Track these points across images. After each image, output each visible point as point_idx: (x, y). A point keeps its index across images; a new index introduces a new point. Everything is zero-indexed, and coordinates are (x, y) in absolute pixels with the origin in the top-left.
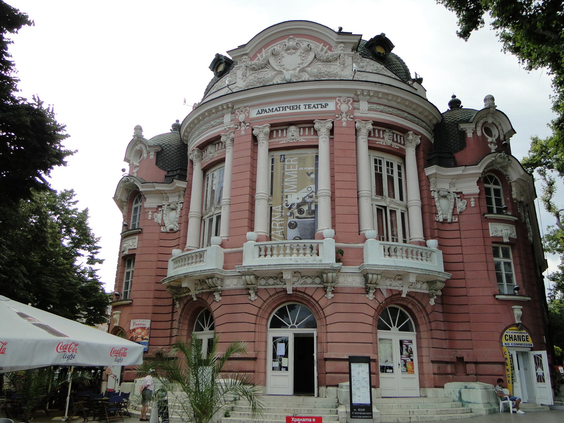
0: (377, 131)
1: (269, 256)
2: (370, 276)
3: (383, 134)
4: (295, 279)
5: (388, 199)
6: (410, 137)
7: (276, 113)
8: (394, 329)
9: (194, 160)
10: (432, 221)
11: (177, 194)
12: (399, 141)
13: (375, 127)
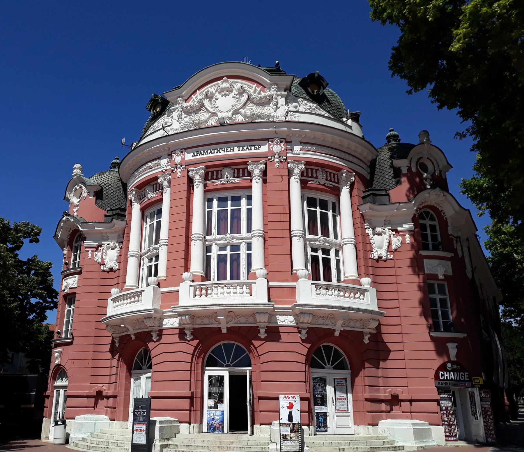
0: (310, 170)
1: (203, 296)
3: (316, 173)
10: (366, 259)
12: (333, 180)
13: (308, 167)
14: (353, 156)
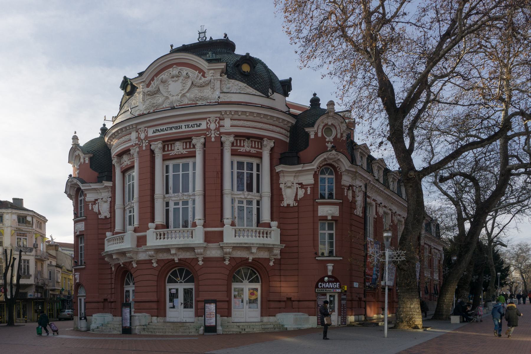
1: (162, 239)
4: (180, 253)
5: (246, 193)
6: (265, 143)
7: (166, 132)
9: (116, 165)
11: (106, 190)
12: (257, 146)
14: (273, 125)
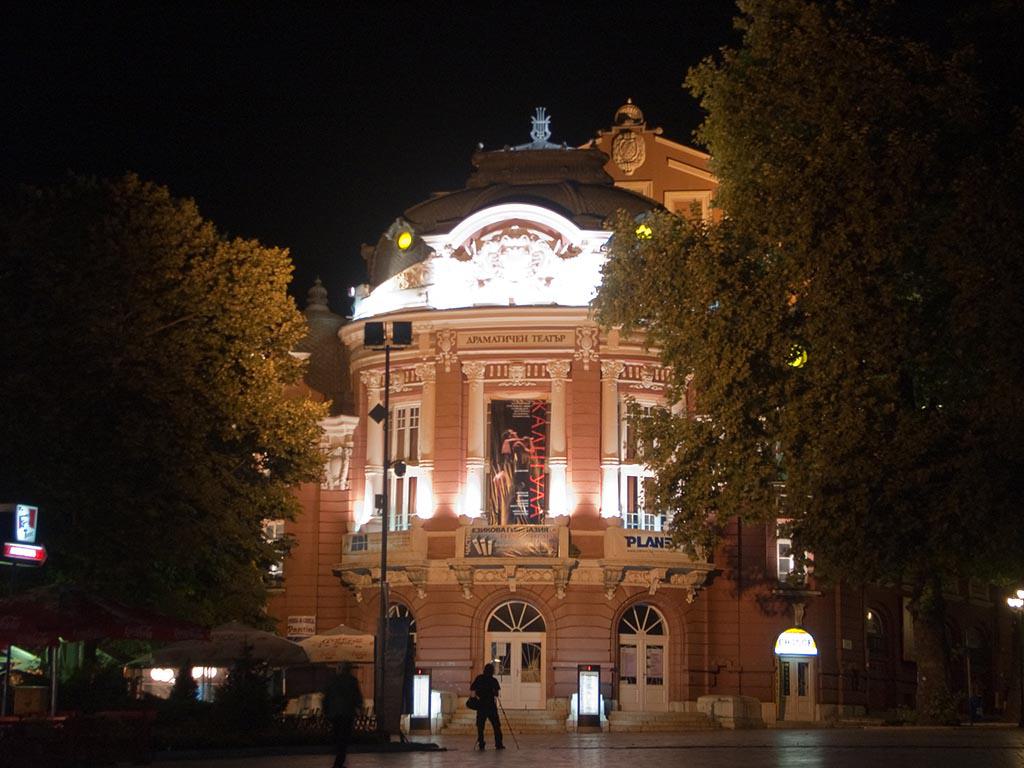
2: (609, 573)
8: (641, 632)
